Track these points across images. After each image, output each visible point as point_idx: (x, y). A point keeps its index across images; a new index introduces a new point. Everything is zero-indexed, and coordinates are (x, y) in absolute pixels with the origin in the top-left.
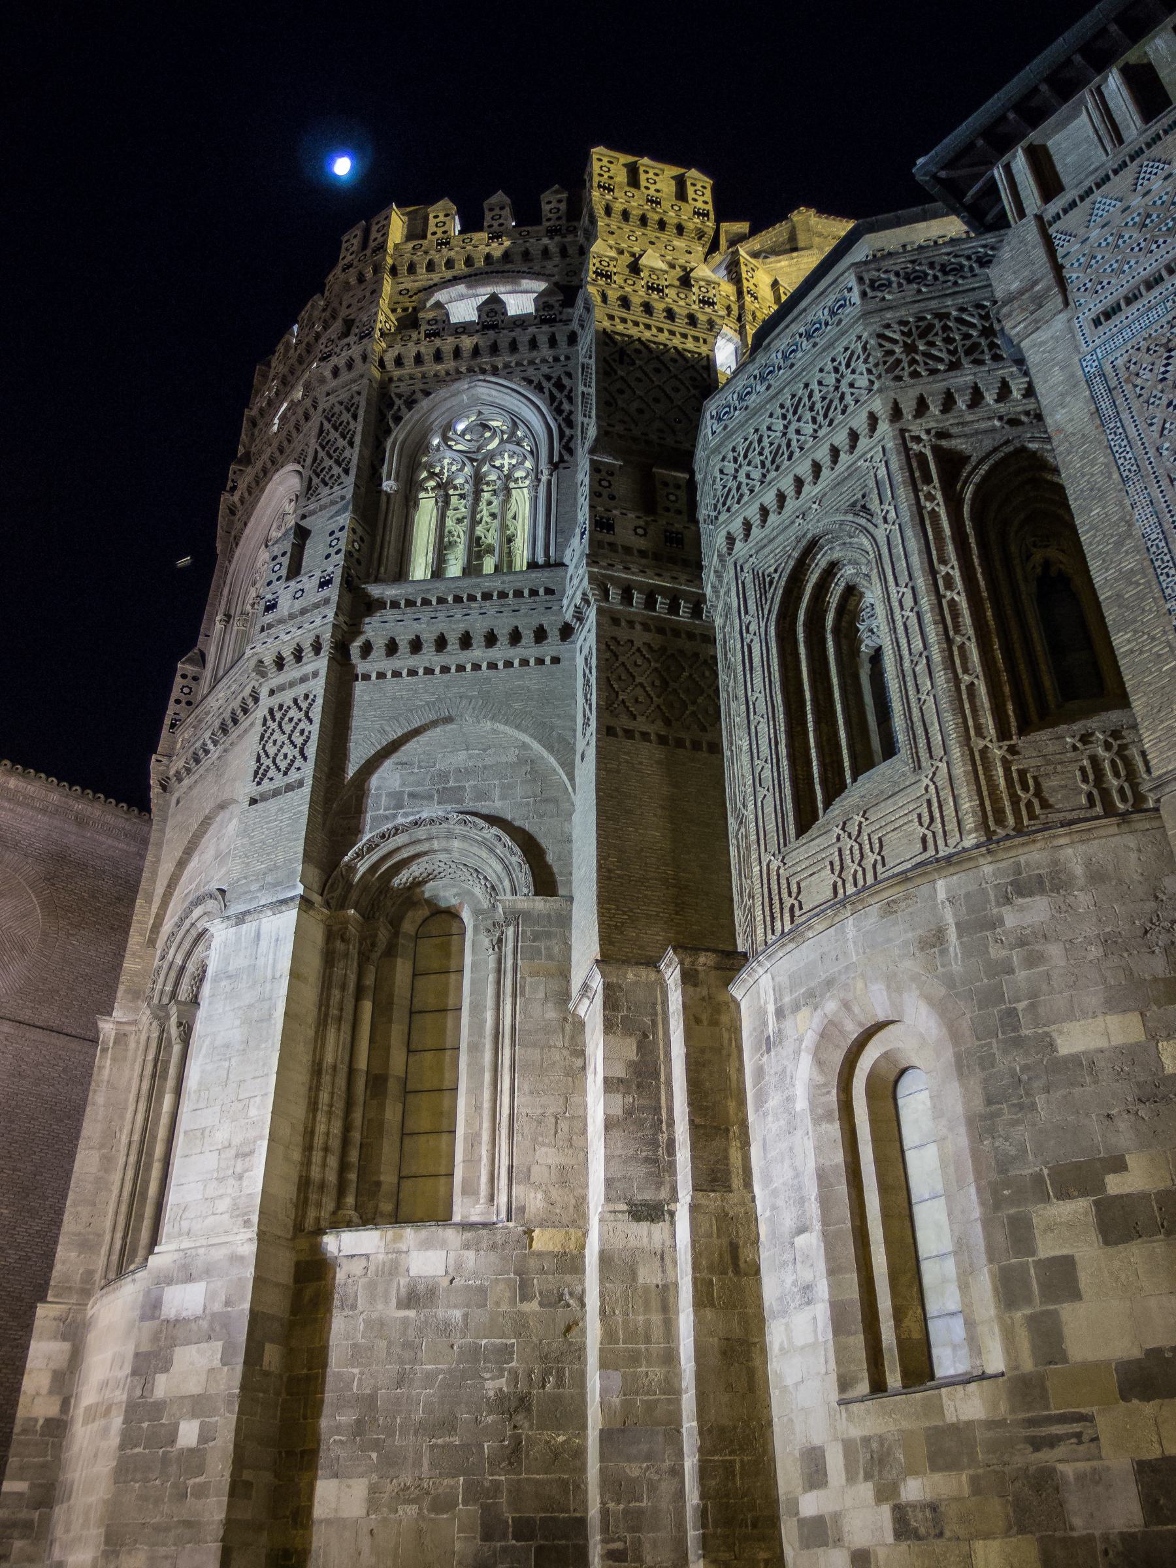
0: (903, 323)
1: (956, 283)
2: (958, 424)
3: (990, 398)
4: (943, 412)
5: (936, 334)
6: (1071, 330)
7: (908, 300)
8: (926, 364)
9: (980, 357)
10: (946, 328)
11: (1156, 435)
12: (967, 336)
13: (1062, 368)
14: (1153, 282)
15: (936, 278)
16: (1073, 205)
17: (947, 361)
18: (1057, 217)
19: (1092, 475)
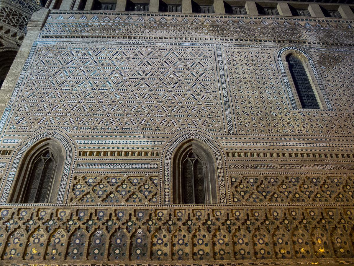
0: (11, 9)
1: (29, 11)
2: (6, 37)
3: (17, 37)
4: (5, 33)
5: (16, 17)
6: (38, 35)
7: (16, 6)
8: (9, 21)
9: (22, 28)
10: (19, 18)
11: (35, 64)
12: (22, 22)
13: (31, 41)
14: (57, 37)
15: (26, 7)
16: (57, 13)
17: (14, 24)
18: (53, 13)
19: (19, 64)
